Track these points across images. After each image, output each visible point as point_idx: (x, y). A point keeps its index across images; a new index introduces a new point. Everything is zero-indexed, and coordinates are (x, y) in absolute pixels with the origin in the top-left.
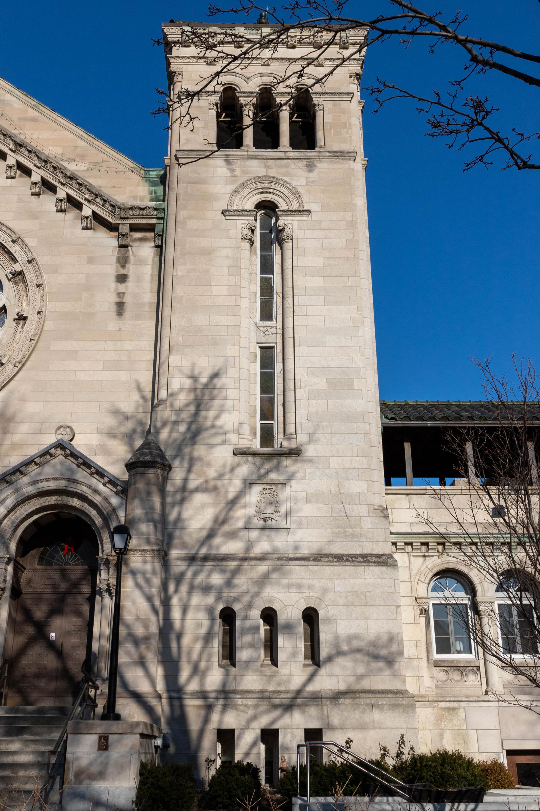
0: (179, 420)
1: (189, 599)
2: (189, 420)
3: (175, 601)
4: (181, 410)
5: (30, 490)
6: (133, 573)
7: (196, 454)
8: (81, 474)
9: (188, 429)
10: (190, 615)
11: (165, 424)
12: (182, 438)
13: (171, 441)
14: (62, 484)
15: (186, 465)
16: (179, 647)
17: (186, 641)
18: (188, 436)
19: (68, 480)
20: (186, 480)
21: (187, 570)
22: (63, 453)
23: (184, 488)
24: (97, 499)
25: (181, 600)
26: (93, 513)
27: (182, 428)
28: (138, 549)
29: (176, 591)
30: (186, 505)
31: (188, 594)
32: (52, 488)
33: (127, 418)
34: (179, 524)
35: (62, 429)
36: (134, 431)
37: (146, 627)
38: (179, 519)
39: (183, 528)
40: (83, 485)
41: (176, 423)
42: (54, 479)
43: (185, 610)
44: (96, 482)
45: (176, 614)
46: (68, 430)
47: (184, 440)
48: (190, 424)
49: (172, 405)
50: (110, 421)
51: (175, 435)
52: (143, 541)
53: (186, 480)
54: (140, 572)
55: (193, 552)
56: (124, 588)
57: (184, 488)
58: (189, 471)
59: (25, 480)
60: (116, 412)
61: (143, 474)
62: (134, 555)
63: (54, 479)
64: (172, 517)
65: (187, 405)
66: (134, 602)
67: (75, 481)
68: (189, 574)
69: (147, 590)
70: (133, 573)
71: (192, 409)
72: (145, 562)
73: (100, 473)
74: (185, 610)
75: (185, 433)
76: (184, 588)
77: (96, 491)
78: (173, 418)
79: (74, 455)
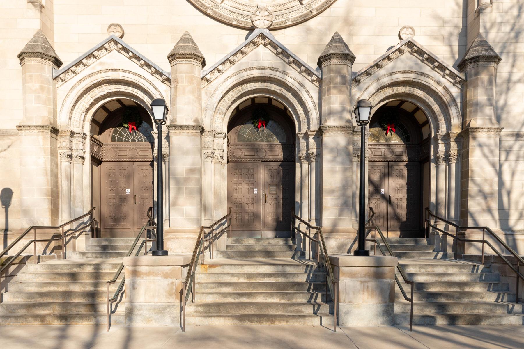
0: (504, 21)
1: (516, 166)
2: (512, 21)
3: (506, 168)
4: (506, 12)
5: (386, 80)
6: (480, 146)
7: (518, 51)
8: (427, 69)
9: (512, 29)
10: (517, 177)
11: (492, 25)
12: (507, 37)
13: (498, 40)
14: (411, 76)
15: (511, 60)
16: (509, 200)
17: (514, 195)
18: (513, 34)
19: (415, 73)
20: (511, 74)
21: (514, 144)
22: (410, 50)
23: (509, 80)
24: (440, 90)
25: (510, 166)
26: (431, 101)
27: (507, 28)
28: (484, 127)
29: (506, 159)
30: (511, 94)
31: (516, 163)
32: (402, 79)
33: (445, 22)
34: (506, 109)
35: (405, 29)
36: (451, 35)
37: (491, 186)
38: (505, 104)
39: (508, 112)
40: (428, 77)
41: (501, 24)
42: (404, 72)
43: (513, 174)
44: (437, 75)
45: (507, 177)
46: (410, 30)
47: (508, 39)
48: (514, 25)
49: (498, 8)
50: (434, 25)
51: (501, 34)
52: (488, 122)
53: (511, 74)
54: (486, 146)
55: (516, 130)
56: (472, 157)
57: (509, 80)
58: (513, 66)
59: (382, 72)
60: (437, 17)
61: (486, 67)
62: (479, 132)
63: (404, 72)
64: (501, 103)
65: (511, 8)
66: (482, 168)
67: (422, 74)
68: (516, 148)
69: (491, 158)
70: (480, 146)
71: (515, 12)
72: (489, 137)
73: (442, 68)
74: (513, 174)
75: (509, 33)
76: (512, 157)
77: (438, 83)
78: (499, 20)
79: (420, 52)
